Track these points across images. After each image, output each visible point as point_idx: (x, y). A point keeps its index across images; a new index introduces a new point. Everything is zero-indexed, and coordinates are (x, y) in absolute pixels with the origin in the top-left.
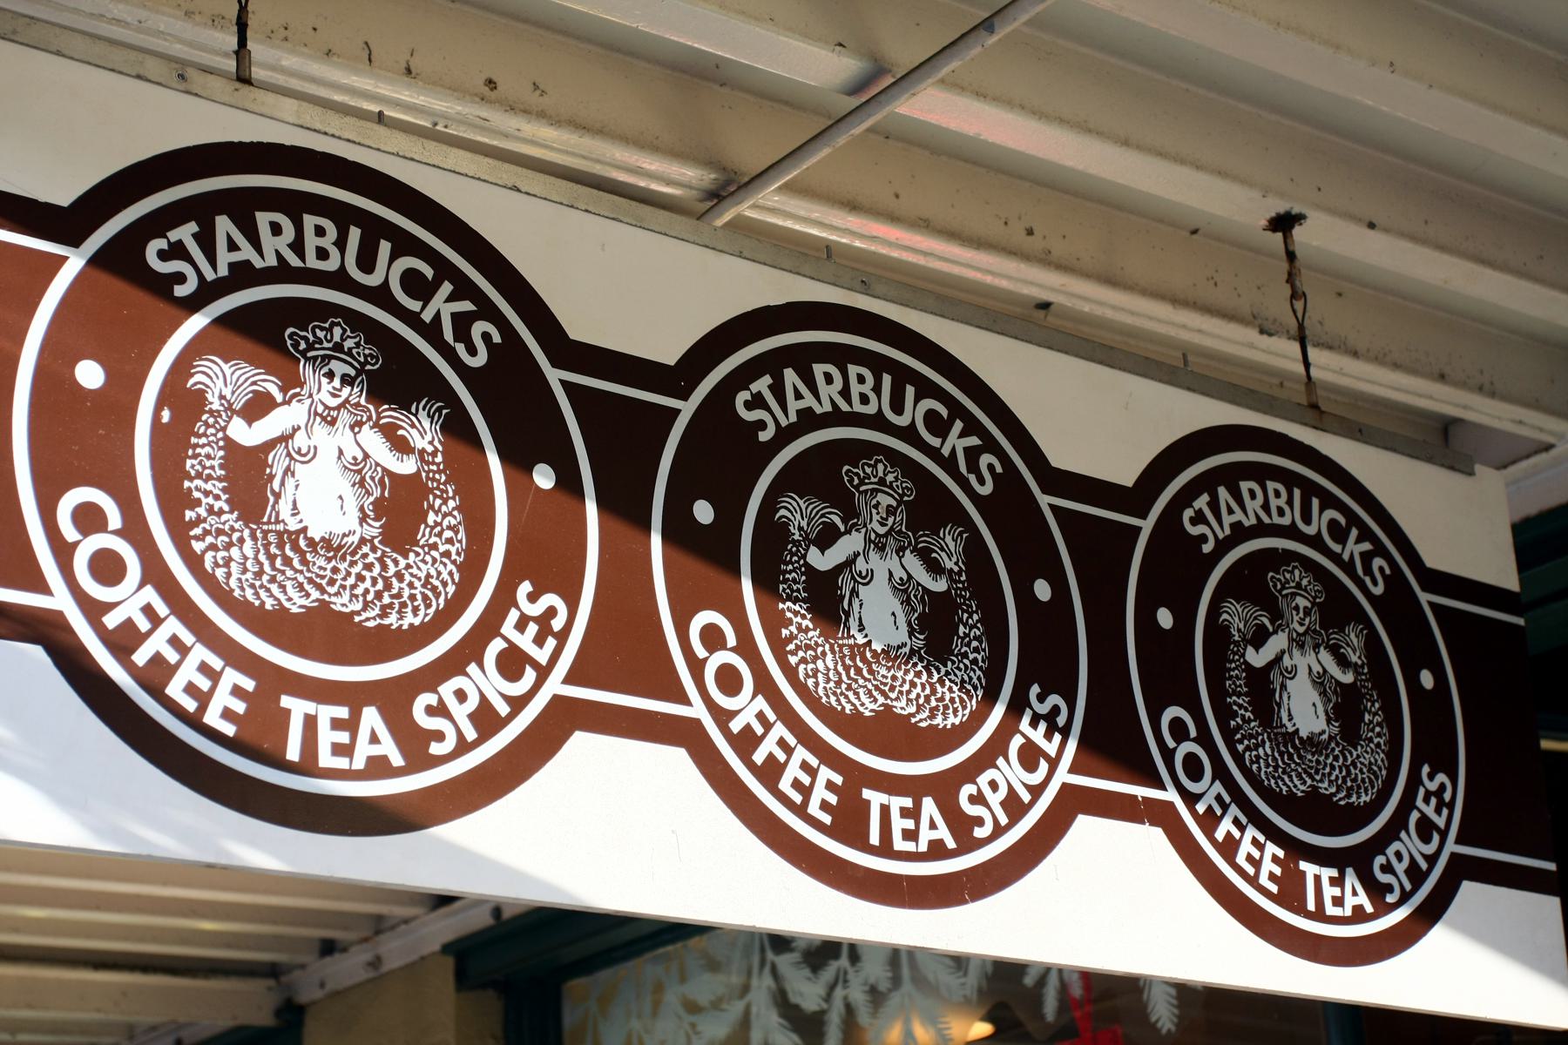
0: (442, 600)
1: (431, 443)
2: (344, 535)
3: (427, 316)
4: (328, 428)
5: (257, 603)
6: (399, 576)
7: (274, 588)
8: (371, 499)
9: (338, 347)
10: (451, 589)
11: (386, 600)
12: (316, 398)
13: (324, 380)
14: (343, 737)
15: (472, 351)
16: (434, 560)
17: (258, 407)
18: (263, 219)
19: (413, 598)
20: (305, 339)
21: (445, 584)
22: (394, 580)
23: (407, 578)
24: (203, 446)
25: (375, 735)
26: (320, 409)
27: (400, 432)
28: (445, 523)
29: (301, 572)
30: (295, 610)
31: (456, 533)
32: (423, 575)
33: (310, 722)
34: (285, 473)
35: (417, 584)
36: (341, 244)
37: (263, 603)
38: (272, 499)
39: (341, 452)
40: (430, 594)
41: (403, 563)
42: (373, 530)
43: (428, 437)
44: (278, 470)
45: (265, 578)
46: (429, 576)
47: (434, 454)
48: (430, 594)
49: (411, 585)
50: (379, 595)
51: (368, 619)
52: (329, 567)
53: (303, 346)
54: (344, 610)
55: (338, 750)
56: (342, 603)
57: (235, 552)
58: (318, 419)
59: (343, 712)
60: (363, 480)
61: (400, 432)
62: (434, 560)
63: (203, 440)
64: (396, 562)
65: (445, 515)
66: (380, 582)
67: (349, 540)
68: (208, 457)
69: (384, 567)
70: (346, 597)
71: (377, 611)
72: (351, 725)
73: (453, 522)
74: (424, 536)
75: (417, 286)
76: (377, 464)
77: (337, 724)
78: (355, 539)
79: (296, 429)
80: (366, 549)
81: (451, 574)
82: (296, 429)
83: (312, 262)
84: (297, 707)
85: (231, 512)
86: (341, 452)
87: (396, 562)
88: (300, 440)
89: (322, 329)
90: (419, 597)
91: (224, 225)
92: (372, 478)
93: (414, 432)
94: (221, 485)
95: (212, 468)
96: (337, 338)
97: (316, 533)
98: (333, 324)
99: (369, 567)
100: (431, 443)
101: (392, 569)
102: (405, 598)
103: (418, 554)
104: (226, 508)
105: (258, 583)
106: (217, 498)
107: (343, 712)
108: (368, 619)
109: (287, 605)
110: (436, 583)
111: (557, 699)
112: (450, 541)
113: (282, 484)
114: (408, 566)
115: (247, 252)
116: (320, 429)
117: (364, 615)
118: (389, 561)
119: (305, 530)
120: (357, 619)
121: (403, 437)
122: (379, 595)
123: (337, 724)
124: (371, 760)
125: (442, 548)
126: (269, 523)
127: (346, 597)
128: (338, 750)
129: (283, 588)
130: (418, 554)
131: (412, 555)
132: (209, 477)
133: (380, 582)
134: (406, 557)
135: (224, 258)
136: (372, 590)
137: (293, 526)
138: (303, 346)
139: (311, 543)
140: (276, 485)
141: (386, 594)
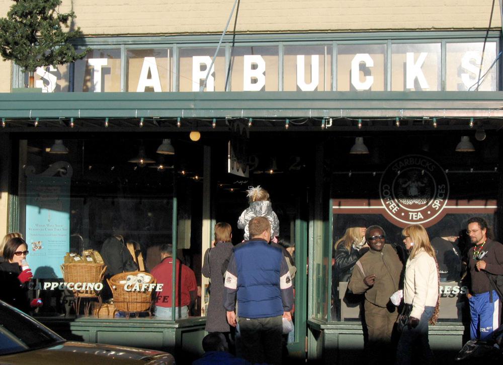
14: (416, 216)
15: (431, 169)
17: (405, 183)
18: (405, 160)
25: (420, 216)
33: (412, 215)
42: (419, 194)
55: (416, 218)
59: (416, 214)
72: (417, 215)
75: (424, 163)
77: (415, 215)
84: (411, 214)
88: (411, 185)
91: (400, 162)
107: (416, 214)
111: (444, 209)
116: (413, 183)
123: (415, 215)
124: (419, 219)
128: (416, 218)
135: (400, 166)
137: (410, 195)
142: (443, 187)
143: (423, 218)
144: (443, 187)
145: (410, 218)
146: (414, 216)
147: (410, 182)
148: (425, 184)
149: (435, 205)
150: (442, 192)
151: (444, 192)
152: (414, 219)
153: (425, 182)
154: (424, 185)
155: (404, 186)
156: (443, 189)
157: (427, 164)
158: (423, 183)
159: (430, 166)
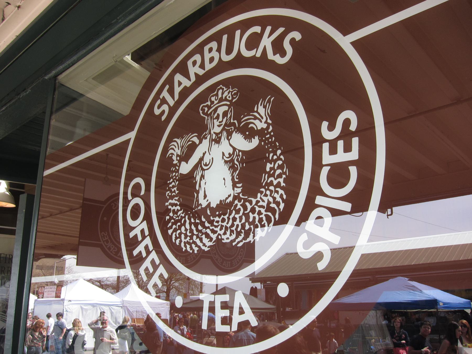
0: (277, 216)
1: (266, 122)
2: (227, 198)
3: (258, 55)
4: (217, 145)
5: (191, 251)
6: (253, 210)
7: (198, 241)
8: (237, 172)
9: (221, 100)
10: (282, 206)
11: (247, 227)
12: (212, 132)
13: (215, 121)
15: (283, 54)
16: (271, 191)
19: (261, 220)
20: (207, 106)
21: (278, 204)
22: (250, 214)
23: (257, 209)
24: (171, 183)
26: (214, 136)
27: (251, 125)
28: (276, 165)
29: (208, 228)
30: (206, 249)
31: (282, 169)
32: (265, 204)
34: (201, 180)
35: (263, 210)
36: (219, 50)
37: (194, 251)
38: (196, 195)
39: (223, 154)
40: (270, 214)
41: (254, 201)
43: (264, 120)
44: (198, 178)
45: (195, 237)
46: (269, 203)
47: (268, 128)
48: (270, 214)
49: (260, 213)
50: (243, 226)
51: (238, 243)
52: (220, 220)
53: (206, 109)
54: (228, 241)
56: (227, 238)
57: (183, 228)
58: (213, 142)
60: (234, 164)
61: (251, 125)
62: (271, 191)
63: (172, 180)
64: (251, 202)
65: (275, 161)
66: (244, 217)
67: (228, 201)
68: (173, 187)
69: (245, 208)
70: (228, 233)
71: (243, 235)
73: (280, 162)
74: (265, 179)
75: (253, 42)
76: (240, 151)
78: (231, 199)
79: (204, 154)
80: (236, 202)
81: (281, 196)
82: (204, 154)
83: (208, 67)
85: (181, 210)
86: (223, 154)
87: (251, 202)
88: (207, 160)
89: (213, 96)
90: (264, 219)
91: (178, 77)
92: (237, 160)
93: (257, 122)
94: (177, 198)
95: (175, 192)
96: (220, 96)
97: (213, 205)
98: (219, 90)
99: (238, 212)
100: (266, 122)
101: (249, 207)
102: (257, 222)
103: (262, 193)
104: (178, 208)
105: (191, 241)
106: (176, 205)
108: (238, 243)
109: (203, 248)
110: (273, 205)
112: (280, 176)
113: (200, 186)
114: (258, 202)
115: (187, 83)
117: (237, 240)
118: (247, 204)
119: (209, 204)
120: (234, 244)
121: (252, 127)
122: (243, 226)
125: (275, 182)
126: (196, 207)
127: (228, 233)
129: (201, 240)
130: (262, 193)
131: (259, 195)
132: (174, 196)
133: (244, 217)
134: (256, 197)
136: (240, 224)
137: (204, 203)
138: (206, 109)
139: (212, 209)
140: (197, 188)
141: (247, 224)
142: (347, 122)
143: (254, 322)
144: (347, 122)
145: (204, 326)
146: (220, 314)
147: (206, 142)
148: (261, 133)
149: (314, 239)
150: (342, 156)
151: (354, 155)
152: (220, 328)
153: (260, 125)
154: (255, 142)
155: (185, 168)
156: (346, 135)
157: (266, 42)
158: (250, 134)
159: (278, 46)
